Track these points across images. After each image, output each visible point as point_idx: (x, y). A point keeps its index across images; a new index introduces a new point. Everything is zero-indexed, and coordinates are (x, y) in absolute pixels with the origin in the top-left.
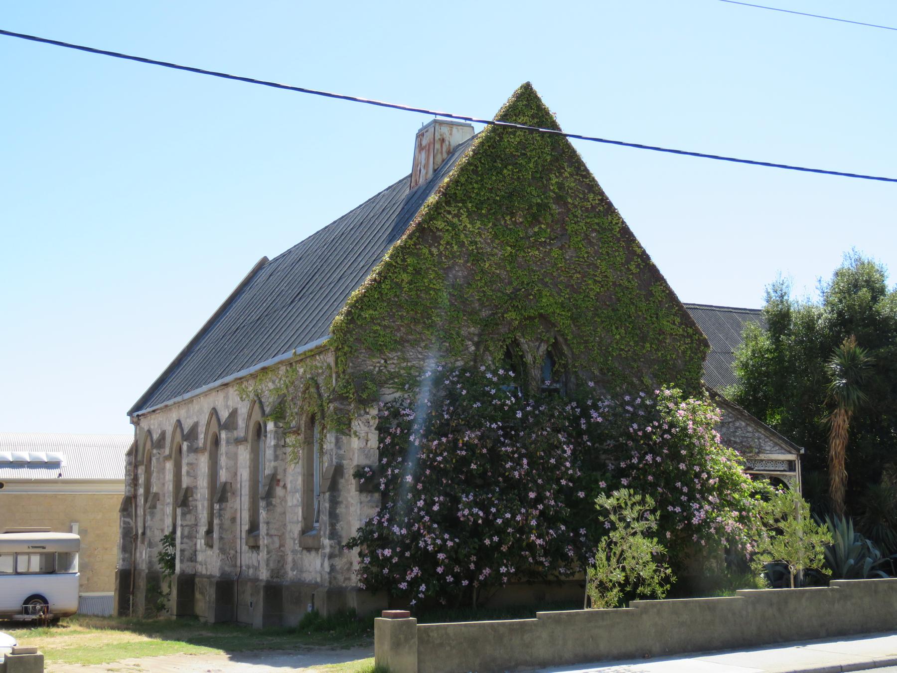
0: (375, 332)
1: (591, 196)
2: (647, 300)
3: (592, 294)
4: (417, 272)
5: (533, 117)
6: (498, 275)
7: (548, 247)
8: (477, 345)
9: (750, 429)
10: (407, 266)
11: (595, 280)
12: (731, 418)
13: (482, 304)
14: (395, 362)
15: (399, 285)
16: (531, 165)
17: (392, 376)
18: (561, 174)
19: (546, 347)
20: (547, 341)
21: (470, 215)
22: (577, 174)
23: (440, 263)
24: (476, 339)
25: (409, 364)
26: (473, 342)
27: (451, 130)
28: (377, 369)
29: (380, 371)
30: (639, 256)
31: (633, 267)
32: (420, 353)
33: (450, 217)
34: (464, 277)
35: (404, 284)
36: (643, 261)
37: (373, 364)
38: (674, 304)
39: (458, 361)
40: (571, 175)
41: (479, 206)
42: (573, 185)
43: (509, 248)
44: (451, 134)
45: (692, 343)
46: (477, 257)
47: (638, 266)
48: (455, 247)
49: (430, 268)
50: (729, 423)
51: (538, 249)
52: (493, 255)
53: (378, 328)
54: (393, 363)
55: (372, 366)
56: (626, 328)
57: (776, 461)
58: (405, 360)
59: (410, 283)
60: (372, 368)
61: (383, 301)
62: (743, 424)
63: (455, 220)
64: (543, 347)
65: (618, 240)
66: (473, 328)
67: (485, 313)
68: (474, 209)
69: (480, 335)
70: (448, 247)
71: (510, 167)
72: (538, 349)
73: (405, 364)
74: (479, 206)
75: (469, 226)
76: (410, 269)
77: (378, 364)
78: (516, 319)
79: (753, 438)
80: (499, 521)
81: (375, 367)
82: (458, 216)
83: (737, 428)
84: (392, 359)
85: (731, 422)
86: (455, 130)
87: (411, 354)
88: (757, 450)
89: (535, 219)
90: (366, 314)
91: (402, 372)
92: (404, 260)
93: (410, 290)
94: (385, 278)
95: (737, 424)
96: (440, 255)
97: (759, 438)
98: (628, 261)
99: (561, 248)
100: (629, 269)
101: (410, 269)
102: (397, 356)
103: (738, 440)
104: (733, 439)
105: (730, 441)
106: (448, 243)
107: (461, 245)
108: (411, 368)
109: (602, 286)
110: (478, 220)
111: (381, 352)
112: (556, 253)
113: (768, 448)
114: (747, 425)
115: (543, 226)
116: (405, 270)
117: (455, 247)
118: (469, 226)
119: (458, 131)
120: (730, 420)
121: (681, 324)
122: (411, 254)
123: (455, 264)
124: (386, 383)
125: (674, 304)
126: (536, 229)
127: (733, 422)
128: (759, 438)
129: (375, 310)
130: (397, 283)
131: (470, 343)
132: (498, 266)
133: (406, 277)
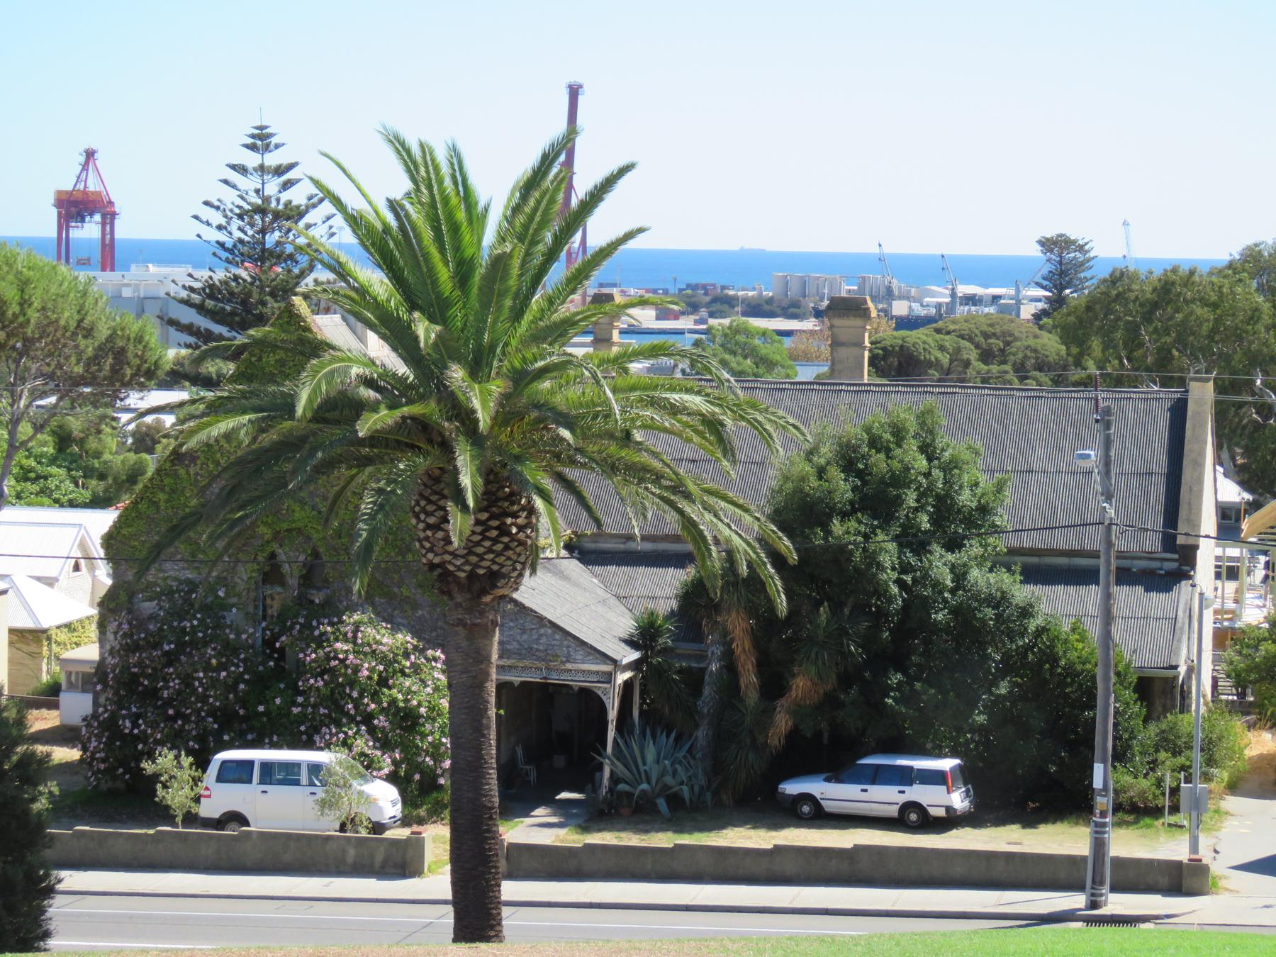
4: (173, 491)
9: (557, 637)
15: (156, 504)
20: (304, 551)
23: (197, 481)
35: (162, 503)
50: (531, 629)
57: (590, 672)
58: (161, 570)
59: (167, 501)
61: (142, 519)
62: (550, 631)
76: (167, 489)
79: (561, 646)
83: (542, 635)
88: (564, 659)
91: (159, 581)
92: (162, 481)
93: (167, 508)
94: (142, 499)
95: (542, 631)
96: (197, 474)
97: (568, 647)
101: (167, 489)
103: (541, 648)
105: (531, 648)
106: (202, 464)
108: (166, 579)
113: (578, 657)
114: (554, 632)
116: (162, 490)
127: (537, 629)
128: (568, 647)
133: (162, 496)
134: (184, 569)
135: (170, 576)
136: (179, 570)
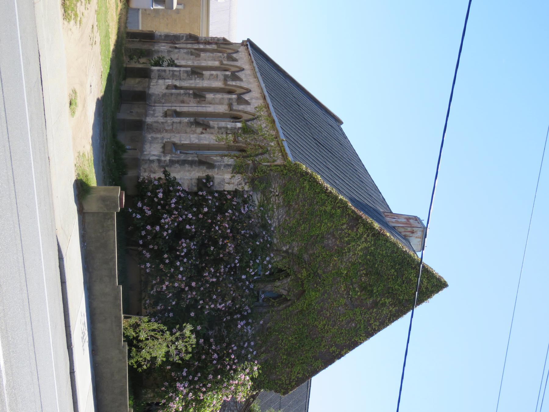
0: (295, 189)
1: (377, 324)
2: (313, 357)
3: (317, 323)
4: (332, 216)
5: (427, 288)
6: (329, 265)
7: (346, 296)
8: (287, 252)
10: (335, 209)
11: (325, 325)
12: (240, 407)
13: (311, 255)
14: (277, 201)
16: (397, 287)
17: (268, 199)
18: (391, 305)
19: (285, 294)
21: (366, 248)
22: (391, 315)
23: (337, 230)
24: (290, 251)
25: (275, 210)
26: (288, 249)
27: (419, 238)
28: (273, 190)
29: (271, 192)
30: (340, 352)
31: (333, 348)
32: (282, 216)
33: (365, 236)
34: (328, 245)
36: (337, 355)
37: (276, 188)
38: (310, 373)
39: (277, 240)
40: (390, 311)
41: (371, 254)
42: (385, 312)
43: (346, 272)
44: (416, 237)
45: (286, 385)
46: (340, 253)
47: (334, 352)
48: (346, 239)
49: (334, 223)
51: (345, 290)
52: (341, 262)
53: (298, 191)
54: (276, 200)
55: (275, 187)
56: (296, 344)
58: (278, 208)
59: (325, 211)
60: (273, 187)
61: (314, 194)
63: (363, 239)
64: (284, 292)
65: (350, 340)
66: (297, 249)
67: (306, 256)
68: (370, 251)
69: (292, 253)
70: (347, 235)
71: (396, 274)
72: (284, 289)
73: (275, 207)
74: (371, 254)
75: (360, 248)
76: (334, 211)
77: (275, 191)
78: (302, 276)
80: (178, 263)
81: (274, 189)
82: (366, 241)
84: (279, 200)
85: (237, 407)
86: (419, 240)
87: (282, 211)
89: (363, 289)
90: (306, 184)
91: (271, 206)
92: (339, 207)
94: (328, 196)
96: (342, 230)
98: (336, 346)
99: (345, 304)
100: (332, 346)
101: (334, 211)
102: (280, 202)
104: (227, 409)
105: (225, 407)
106: (349, 234)
107: (348, 243)
108: (273, 211)
109: (322, 329)
110: (363, 253)
111: (283, 193)
112: (343, 301)
115: (359, 293)
116: (333, 208)
117: (346, 239)
118: (360, 248)
119: (418, 242)
120: (238, 407)
121: (298, 378)
122: (343, 212)
123: (336, 239)
124: (264, 195)
125: (310, 373)
126: (357, 289)
129: (309, 190)
130: (325, 203)
131: (288, 247)
132: (335, 266)
133: (329, 208)
134: (279, 222)
135: (274, 212)
136: (278, 219)
